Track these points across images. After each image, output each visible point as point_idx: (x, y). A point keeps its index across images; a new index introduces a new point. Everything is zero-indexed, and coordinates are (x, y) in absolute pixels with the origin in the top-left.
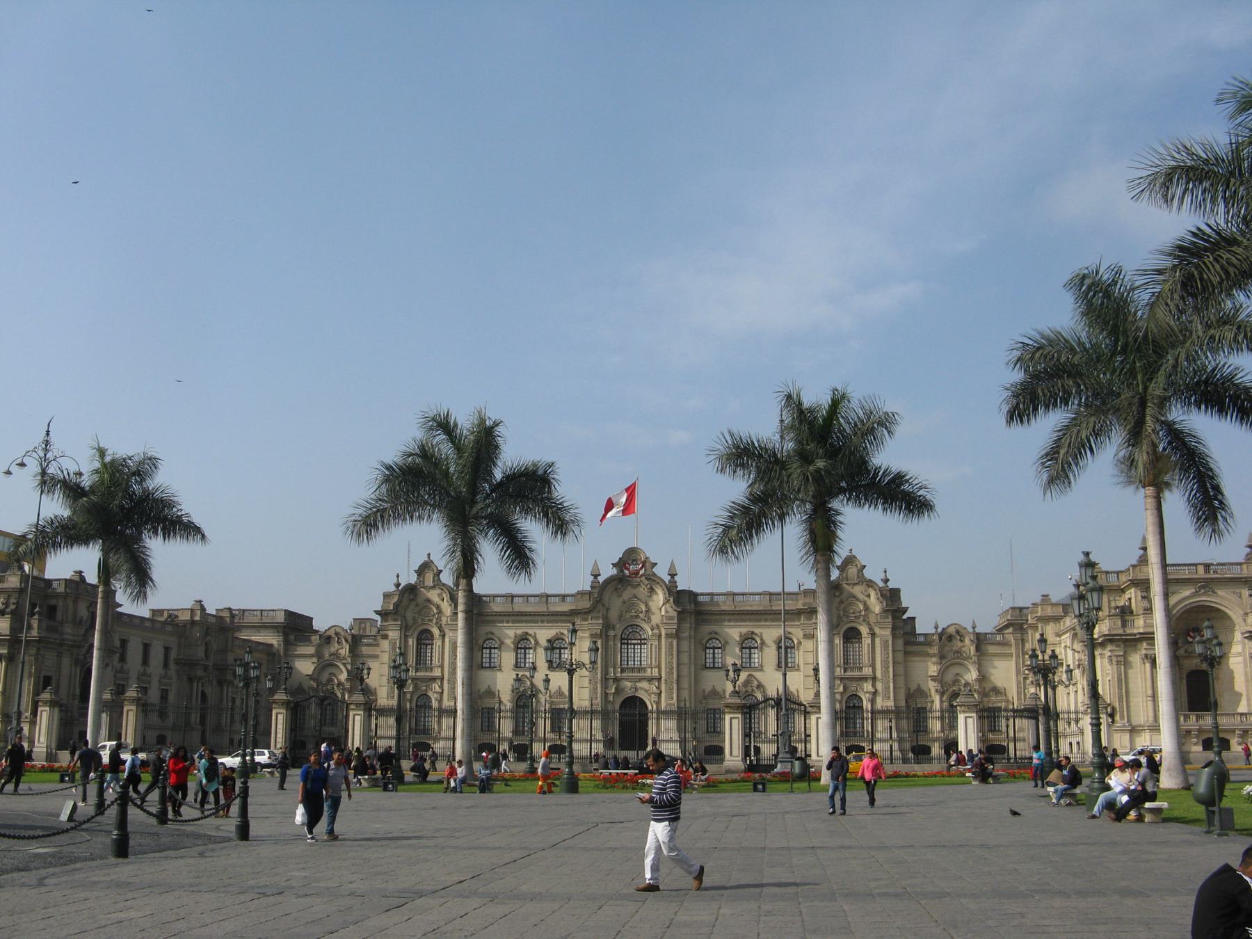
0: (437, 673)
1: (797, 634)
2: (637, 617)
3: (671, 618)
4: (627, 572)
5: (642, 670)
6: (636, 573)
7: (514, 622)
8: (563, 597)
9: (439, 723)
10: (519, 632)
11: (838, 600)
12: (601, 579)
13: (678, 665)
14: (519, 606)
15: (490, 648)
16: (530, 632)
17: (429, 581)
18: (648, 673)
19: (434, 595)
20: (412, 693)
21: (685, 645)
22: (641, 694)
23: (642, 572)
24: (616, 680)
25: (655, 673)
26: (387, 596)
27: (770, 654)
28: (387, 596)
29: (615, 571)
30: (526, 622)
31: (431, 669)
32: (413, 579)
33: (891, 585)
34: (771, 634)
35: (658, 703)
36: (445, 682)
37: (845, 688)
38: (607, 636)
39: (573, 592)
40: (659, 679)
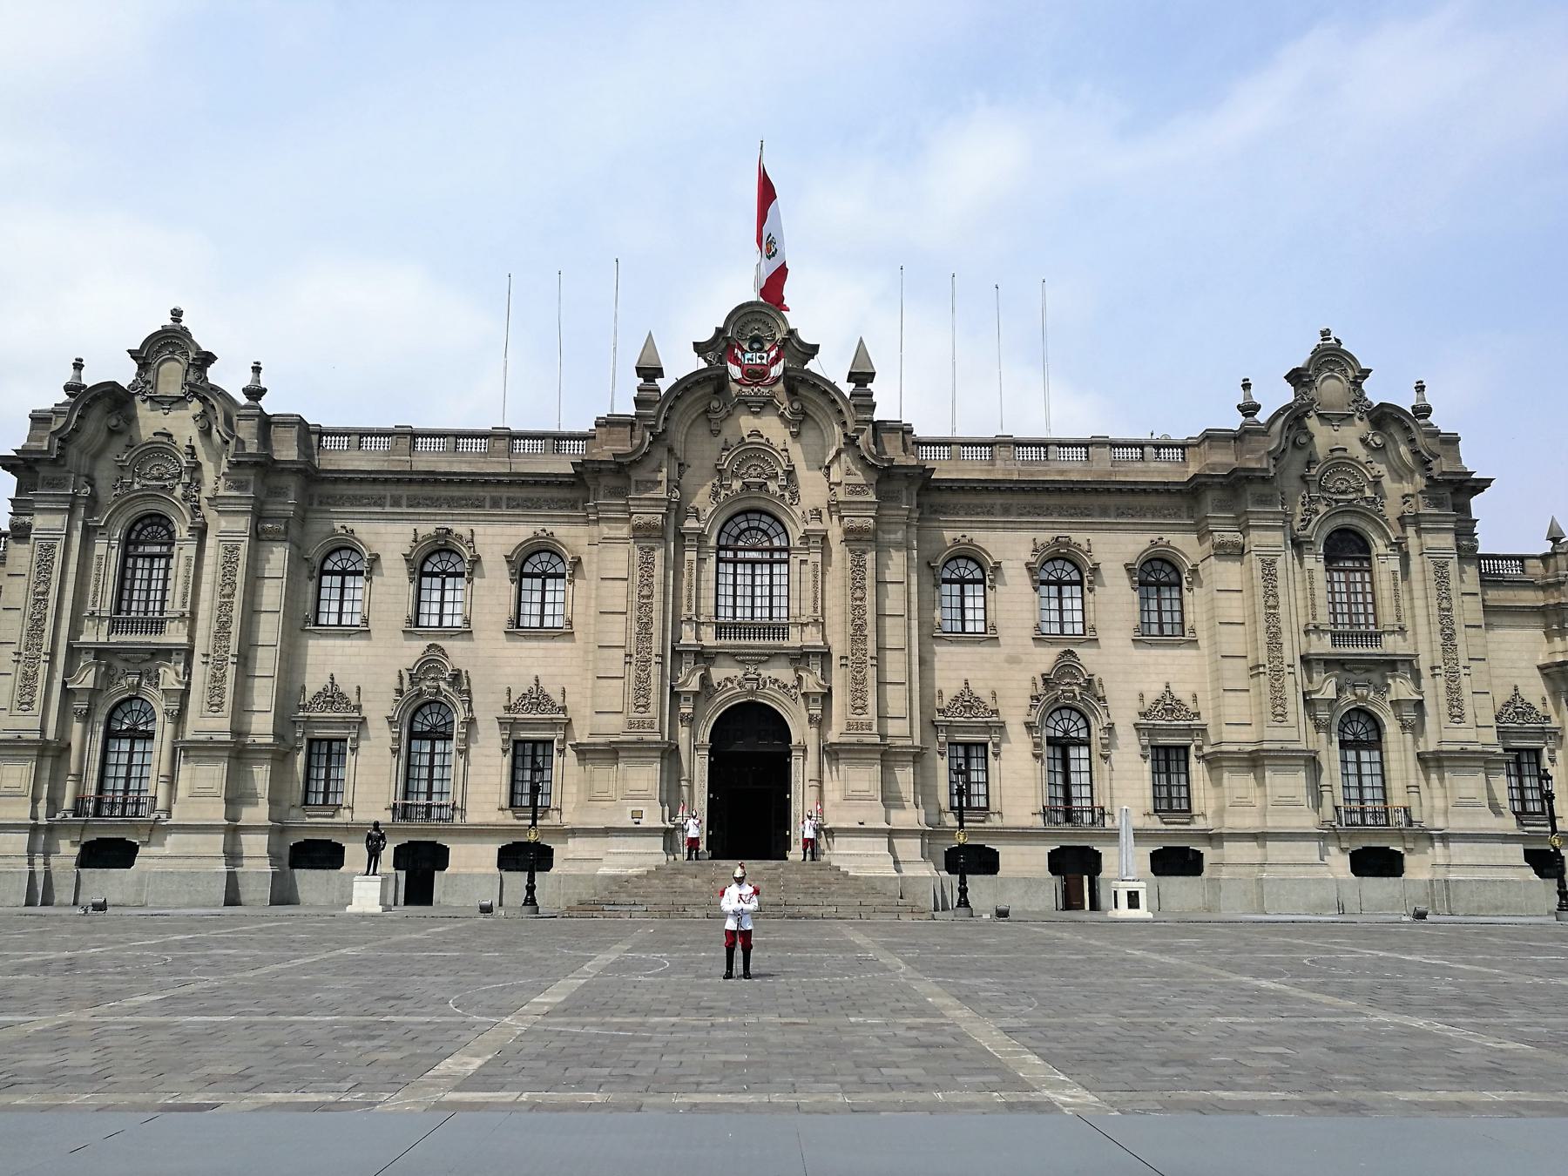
0: (175, 635)
1: (1185, 545)
2: (762, 486)
3: (855, 489)
4: (735, 371)
5: (780, 630)
6: (755, 375)
7: (414, 502)
8: (557, 439)
9: (172, 780)
10: (427, 529)
11: (1301, 457)
12: (664, 384)
13: (880, 616)
14: (429, 458)
15: (344, 573)
16: (460, 529)
17: (171, 378)
18: (795, 639)
19: (183, 425)
20: (94, 693)
21: (896, 565)
22: (773, 698)
23: (776, 371)
24: (704, 657)
25: (812, 638)
26: (38, 419)
27: (1116, 601)
28: (38, 419)
29: (703, 365)
30: (452, 502)
31: (158, 626)
32: (125, 374)
33: (1440, 420)
34: (1115, 548)
35: (821, 723)
36: (197, 659)
37: (1339, 690)
38: (680, 536)
39: (586, 426)
40: (825, 656)
